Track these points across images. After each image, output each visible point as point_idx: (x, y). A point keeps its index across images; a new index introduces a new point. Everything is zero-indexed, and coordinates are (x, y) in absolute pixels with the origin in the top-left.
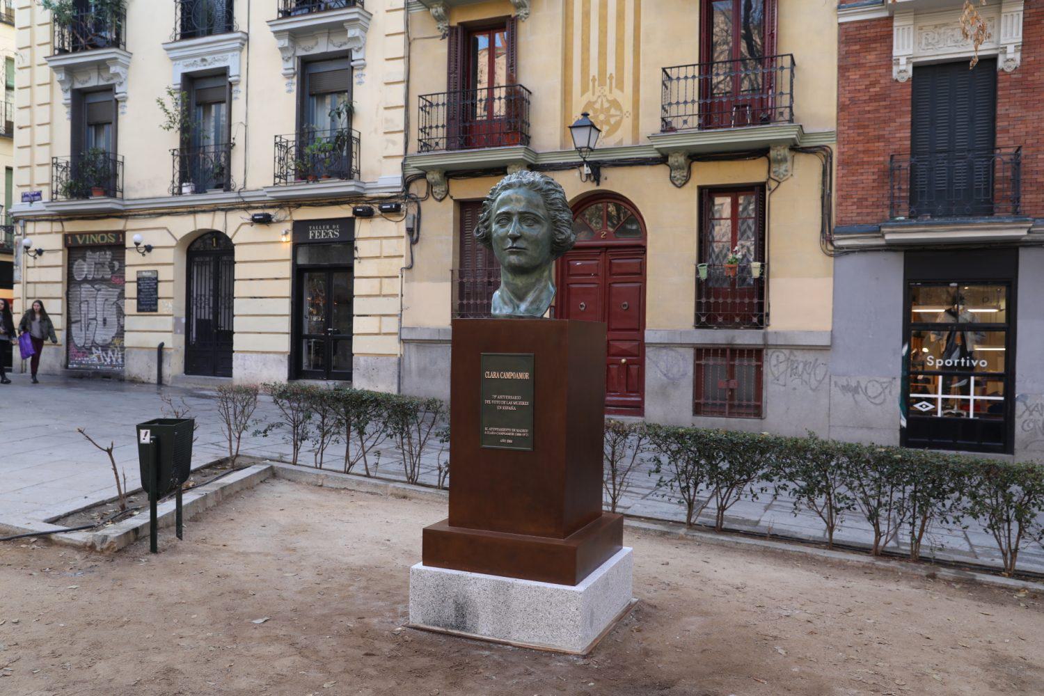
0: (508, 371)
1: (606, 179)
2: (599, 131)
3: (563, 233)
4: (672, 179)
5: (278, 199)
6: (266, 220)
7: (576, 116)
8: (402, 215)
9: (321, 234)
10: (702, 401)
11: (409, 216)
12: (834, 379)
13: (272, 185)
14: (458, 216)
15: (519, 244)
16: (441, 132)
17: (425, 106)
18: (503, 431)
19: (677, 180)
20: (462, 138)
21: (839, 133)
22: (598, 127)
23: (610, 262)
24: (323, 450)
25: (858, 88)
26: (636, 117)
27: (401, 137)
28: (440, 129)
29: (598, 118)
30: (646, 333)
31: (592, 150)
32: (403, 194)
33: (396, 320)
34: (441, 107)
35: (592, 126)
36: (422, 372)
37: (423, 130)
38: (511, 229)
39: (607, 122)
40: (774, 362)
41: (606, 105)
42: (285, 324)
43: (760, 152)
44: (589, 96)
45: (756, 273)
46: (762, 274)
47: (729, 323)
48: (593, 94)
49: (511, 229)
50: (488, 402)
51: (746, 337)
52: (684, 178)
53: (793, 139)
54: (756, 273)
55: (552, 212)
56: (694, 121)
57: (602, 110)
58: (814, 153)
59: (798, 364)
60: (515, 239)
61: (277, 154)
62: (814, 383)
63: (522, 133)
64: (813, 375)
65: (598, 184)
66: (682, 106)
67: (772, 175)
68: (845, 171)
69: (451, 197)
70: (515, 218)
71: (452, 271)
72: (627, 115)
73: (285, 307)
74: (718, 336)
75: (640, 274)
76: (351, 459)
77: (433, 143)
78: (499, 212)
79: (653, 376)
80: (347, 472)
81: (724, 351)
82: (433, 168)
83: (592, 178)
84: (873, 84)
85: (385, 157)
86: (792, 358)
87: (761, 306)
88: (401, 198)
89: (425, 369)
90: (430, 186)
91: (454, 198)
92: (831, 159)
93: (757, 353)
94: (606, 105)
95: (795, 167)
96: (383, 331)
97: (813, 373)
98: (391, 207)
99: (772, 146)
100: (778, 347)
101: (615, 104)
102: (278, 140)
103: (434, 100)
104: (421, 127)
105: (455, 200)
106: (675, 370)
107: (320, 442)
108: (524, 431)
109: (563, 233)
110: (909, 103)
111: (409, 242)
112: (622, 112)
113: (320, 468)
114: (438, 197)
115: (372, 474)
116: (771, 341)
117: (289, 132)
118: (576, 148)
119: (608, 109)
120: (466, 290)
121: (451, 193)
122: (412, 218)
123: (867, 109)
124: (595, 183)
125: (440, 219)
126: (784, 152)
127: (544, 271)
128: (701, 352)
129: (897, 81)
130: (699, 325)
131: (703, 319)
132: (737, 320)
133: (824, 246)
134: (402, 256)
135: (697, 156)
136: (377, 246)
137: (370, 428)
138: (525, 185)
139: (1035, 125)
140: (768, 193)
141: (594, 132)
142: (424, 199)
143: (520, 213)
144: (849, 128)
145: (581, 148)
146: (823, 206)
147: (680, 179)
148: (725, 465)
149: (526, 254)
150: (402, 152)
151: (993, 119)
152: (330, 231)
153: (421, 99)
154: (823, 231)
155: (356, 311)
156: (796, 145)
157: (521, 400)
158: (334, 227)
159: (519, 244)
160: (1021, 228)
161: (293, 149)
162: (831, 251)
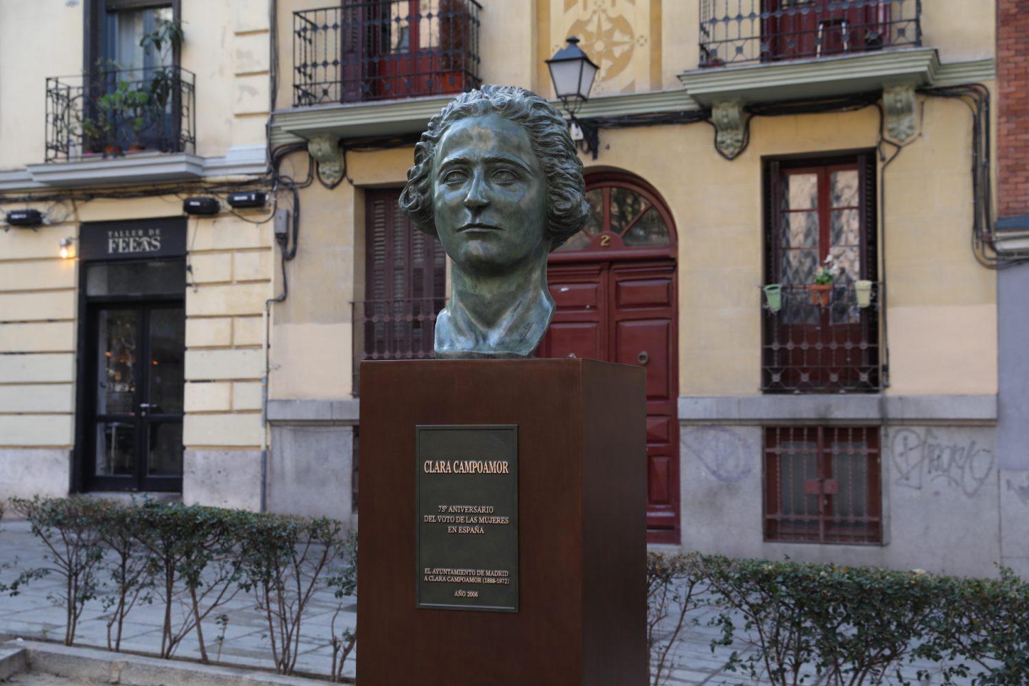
1: (608, 147)
2: (596, 68)
3: (567, 199)
4: (718, 146)
5: (54, 185)
6: (32, 222)
7: (557, 44)
8: (268, 212)
9: (128, 244)
10: (778, 516)
11: (278, 214)
12: (1005, 476)
13: (42, 161)
14: (362, 212)
15: (488, 218)
16: (333, 73)
17: (305, 29)
18: (458, 574)
19: (727, 148)
20: (367, 82)
21: (1000, 62)
22: (595, 62)
23: (618, 288)
24: (122, 616)
26: (657, 45)
27: (265, 81)
28: (331, 68)
29: (595, 49)
30: (681, 402)
31: (585, 100)
32: (269, 177)
33: (258, 387)
34: (331, 32)
35: (585, 59)
36: (304, 474)
37: (302, 69)
38: (470, 191)
39: (608, 54)
40: (899, 448)
41: (606, 26)
42: (66, 399)
43: (865, 97)
44: (577, 12)
46: (874, 300)
47: (819, 384)
48: (585, 7)
49: (470, 191)
50: (430, 518)
51: (849, 407)
53: (922, 74)
54: (864, 299)
55: (545, 159)
56: (754, 49)
57: (599, 34)
59: (942, 451)
60: (477, 209)
61: (50, 110)
62: (971, 485)
63: (468, 74)
64: (967, 470)
65: (595, 157)
66: (733, 24)
67: (887, 136)
68: (1013, 126)
69: (351, 182)
70: (477, 171)
71: (353, 304)
72: (642, 41)
73: (66, 368)
74: (801, 406)
75: (668, 304)
76: (175, 631)
77: (318, 91)
78: (446, 160)
79: (693, 473)
80: (166, 656)
81: (812, 430)
82: (319, 133)
83: (585, 146)
85: (239, 116)
86: (931, 441)
87: (873, 354)
88: (266, 183)
89: (308, 470)
90: (315, 162)
91: (356, 182)
92: (988, 104)
93: (869, 434)
94: (606, 26)
95: (927, 119)
96: (237, 406)
97: (967, 466)
98: (248, 199)
99: (885, 86)
100: (904, 422)
101: (621, 23)
102: (52, 85)
103: (320, 19)
104: (297, 64)
105: (358, 188)
106: (731, 464)
107: (117, 601)
108: (499, 573)
109: (567, 199)
111: (280, 257)
112: (632, 36)
113: (117, 650)
114: (329, 182)
115: (212, 656)
116: (893, 413)
117: (72, 72)
118: (559, 97)
119: (610, 33)
120: (377, 337)
121: (350, 174)
122: (283, 215)
124: (590, 155)
125: (332, 218)
126: (906, 95)
127: (532, 271)
128: (774, 433)
130: (769, 387)
131: (776, 378)
132: (834, 378)
133: (979, 252)
134: (268, 281)
135: (760, 106)
136: (226, 265)
137: (209, 574)
138: (494, 109)
140: (880, 165)
141: (587, 69)
142: (305, 185)
143: (487, 162)
145: (566, 96)
146: (975, 185)
147: (731, 145)
148: (849, 630)
149: (498, 238)
150: (265, 106)
152: (145, 240)
153: (297, 18)
154: (976, 227)
155: (189, 374)
156: (927, 84)
157: (493, 514)
158: (151, 232)
159: (488, 218)
161: (79, 103)
162: (990, 259)
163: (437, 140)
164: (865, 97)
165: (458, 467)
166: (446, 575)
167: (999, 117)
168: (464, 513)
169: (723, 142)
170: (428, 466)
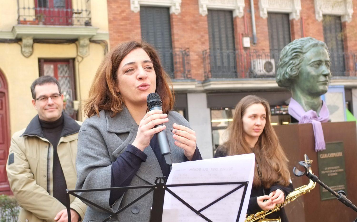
4: (22, 53)
19: (26, 53)
21: (110, 34)
25: (116, 12)
43: (73, 41)
45: (76, 107)
58: (99, 43)
66: (27, 10)
67: (79, 54)
84: (123, 12)
110: (139, 23)
123: (122, 23)
129: (133, 12)
140: (77, 63)
144: (114, 32)
151: (171, 35)
157: (340, 168)
160: (193, 84)
163: (305, 53)
164: (73, 41)
165: (329, 155)
168: (331, 170)
169: (24, 51)
170: (321, 156)
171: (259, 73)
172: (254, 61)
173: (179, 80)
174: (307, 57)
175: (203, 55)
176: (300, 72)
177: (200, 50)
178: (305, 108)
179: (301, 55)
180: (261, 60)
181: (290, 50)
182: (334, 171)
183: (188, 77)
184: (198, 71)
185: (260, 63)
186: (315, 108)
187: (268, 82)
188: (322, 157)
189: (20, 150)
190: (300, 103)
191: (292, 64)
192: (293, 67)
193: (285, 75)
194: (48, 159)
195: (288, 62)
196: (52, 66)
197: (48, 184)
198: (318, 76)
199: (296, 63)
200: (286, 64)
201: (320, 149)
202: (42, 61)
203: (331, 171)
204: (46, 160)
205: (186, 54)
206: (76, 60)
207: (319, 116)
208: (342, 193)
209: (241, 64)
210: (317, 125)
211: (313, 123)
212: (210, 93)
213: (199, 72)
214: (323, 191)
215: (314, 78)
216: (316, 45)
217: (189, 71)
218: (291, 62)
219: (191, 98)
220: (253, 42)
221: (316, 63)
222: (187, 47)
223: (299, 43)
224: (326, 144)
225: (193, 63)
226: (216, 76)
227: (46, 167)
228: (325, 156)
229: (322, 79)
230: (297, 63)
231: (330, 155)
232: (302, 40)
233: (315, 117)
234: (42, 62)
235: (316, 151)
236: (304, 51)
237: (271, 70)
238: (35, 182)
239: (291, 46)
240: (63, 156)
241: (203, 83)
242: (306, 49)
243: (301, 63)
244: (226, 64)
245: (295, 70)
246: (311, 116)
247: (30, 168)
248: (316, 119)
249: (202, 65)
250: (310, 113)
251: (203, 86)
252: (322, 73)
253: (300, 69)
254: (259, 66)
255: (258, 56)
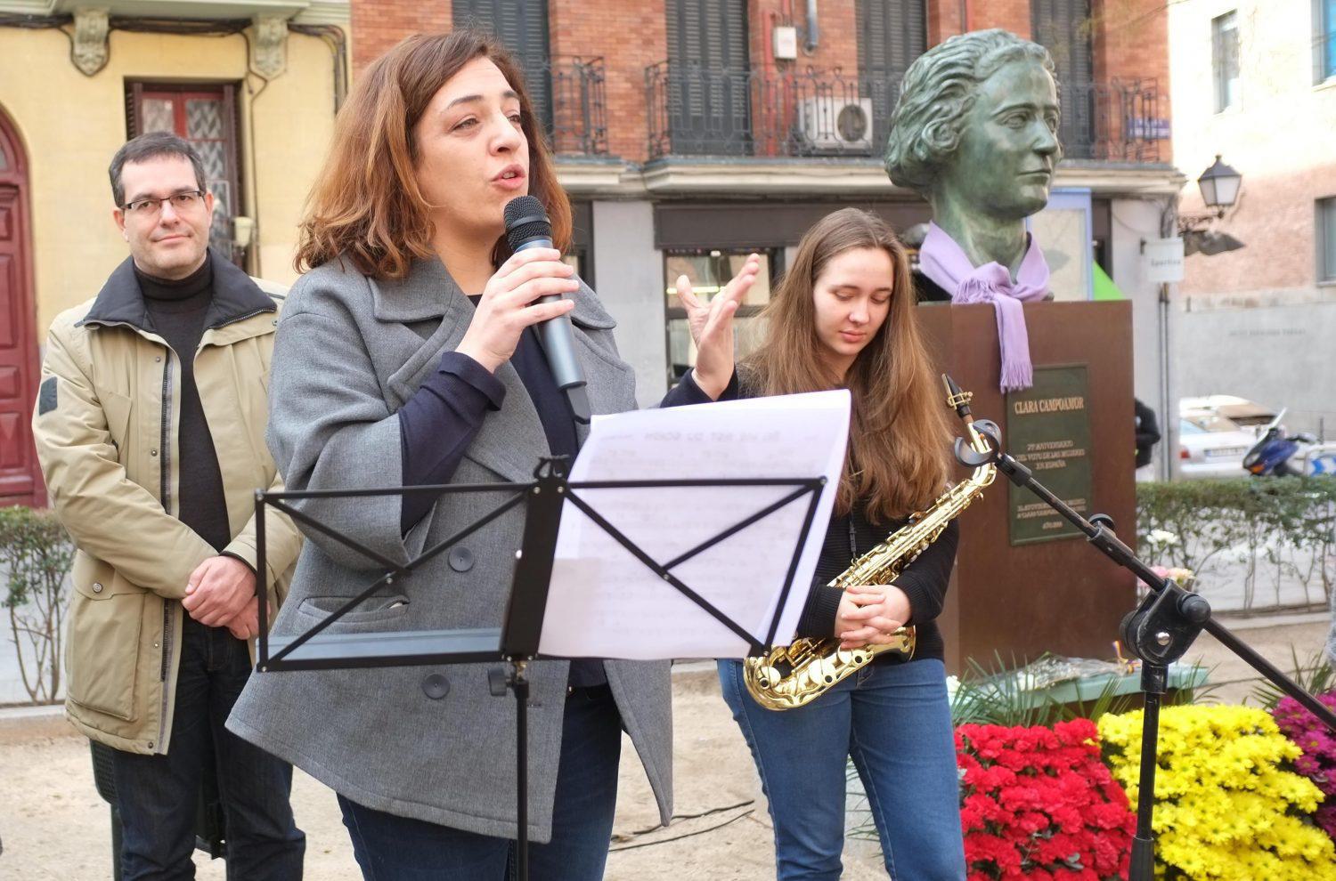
0: (1051, 398)
4: (74, 58)
19: (87, 61)
45: (243, 238)
52: (99, 60)
58: (318, 35)
67: (253, 67)
92: (345, 48)
99: (261, 16)
139: (601, 29)
140: (246, 98)
157: (1074, 448)
160: (613, 173)
163: (982, 80)
165: (1043, 405)
166: (1035, 510)
167: (354, 61)
168: (1048, 450)
169: (81, 56)
170: (1018, 407)
171: (821, 143)
172: (806, 105)
173: (569, 157)
174: (986, 94)
175: (647, 79)
176: (962, 141)
177: (636, 64)
178: (975, 254)
179: (969, 85)
180: (829, 101)
181: (935, 69)
182: (1056, 455)
183: (596, 149)
184: (629, 129)
185: (825, 110)
186: (1005, 255)
187: (848, 170)
188: (1021, 412)
189: (73, 365)
190: (959, 239)
191: (940, 114)
192: (942, 123)
193: (916, 149)
194: (165, 399)
195: (926, 108)
196: (169, 106)
197: (164, 478)
198: (1021, 155)
199: (951, 111)
200: (919, 114)
201: (1015, 384)
202: (138, 87)
203: (1047, 455)
204: (160, 402)
205: (592, 76)
206: (245, 88)
207: (1016, 283)
208: (1105, 521)
209: (764, 111)
210: (1009, 308)
211: (995, 303)
212: (664, 202)
213: (632, 135)
214: (1019, 516)
215: (1006, 161)
216: (1016, 56)
217: (601, 132)
218: (936, 107)
219: (603, 215)
220: (805, 43)
221: (1016, 112)
222: (596, 52)
223: (965, 48)
224: (1035, 370)
225: (613, 106)
226: (685, 150)
227: (157, 425)
228: (1029, 407)
229: (1033, 163)
230: (955, 113)
231: (1046, 406)
232: (973, 39)
233: (1004, 285)
234: (137, 90)
235: (1003, 391)
236: (979, 73)
237: (859, 133)
238: (121, 472)
239: (940, 55)
240: (212, 388)
241: (642, 171)
242: (987, 68)
243: (967, 110)
244: (717, 113)
245: (947, 135)
246: (993, 280)
247: (106, 427)
248: (1005, 289)
249: (643, 114)
250: (988, 271)
251: (644, 180)
252: (1031, 146)
253: (964, 130)
254: (823, 119)
255: (822, 90)
